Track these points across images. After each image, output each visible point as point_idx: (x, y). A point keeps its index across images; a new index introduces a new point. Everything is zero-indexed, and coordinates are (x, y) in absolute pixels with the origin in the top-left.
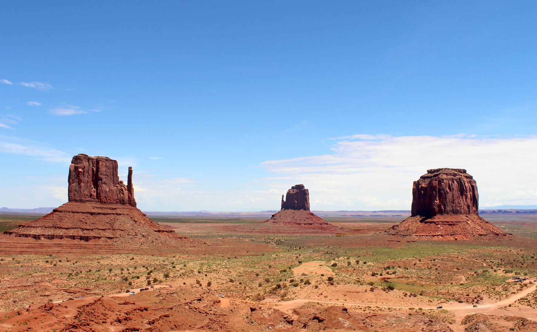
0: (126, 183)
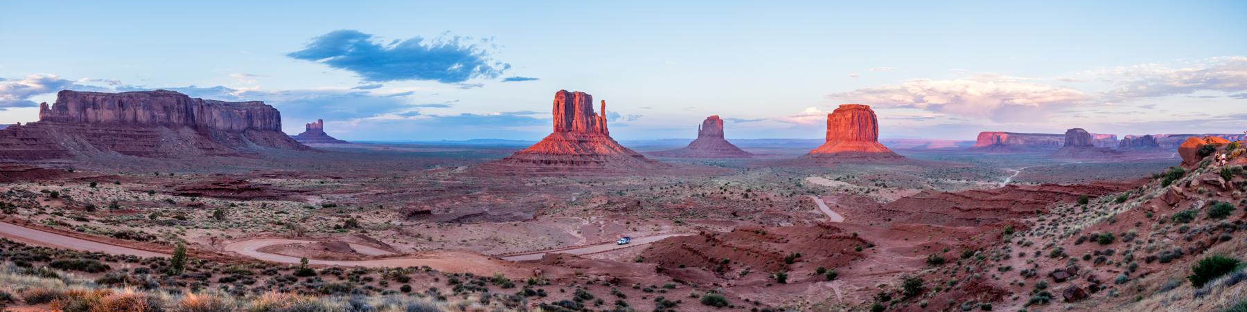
0: (600, 115)
